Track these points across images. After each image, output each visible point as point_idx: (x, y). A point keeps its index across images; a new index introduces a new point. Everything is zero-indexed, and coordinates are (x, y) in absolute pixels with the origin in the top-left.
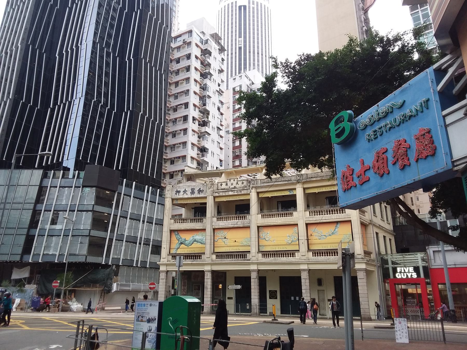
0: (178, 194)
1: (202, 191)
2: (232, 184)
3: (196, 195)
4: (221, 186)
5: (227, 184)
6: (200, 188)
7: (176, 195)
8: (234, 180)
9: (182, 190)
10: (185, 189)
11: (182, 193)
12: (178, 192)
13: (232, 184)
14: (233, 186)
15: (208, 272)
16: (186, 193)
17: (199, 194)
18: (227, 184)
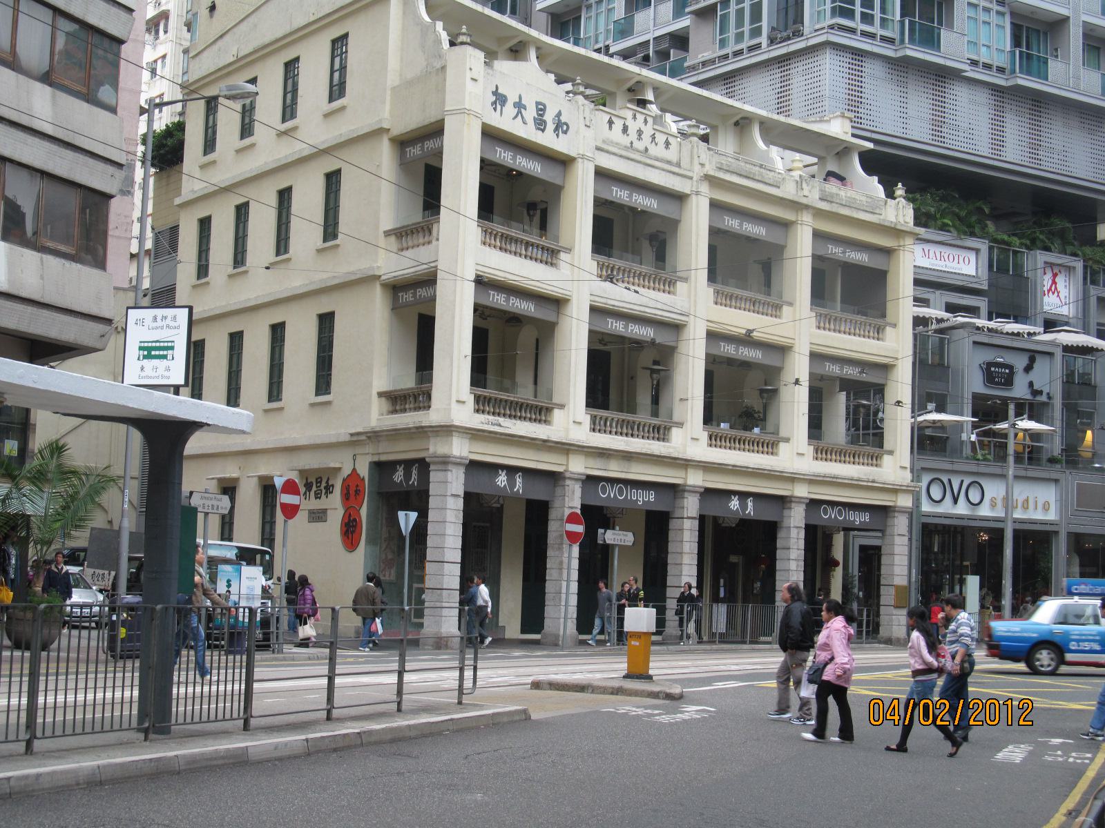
0: (499, 107)
1: (565, 128)
2: (640, 132)
3: (547, 139)
4: (610, 128)
5: (625, 129)
6: (559, 114)
7: (495, 109)
8: (646, 122)
9: (512, 99)
10: (520, 97)
11: (509, 109)
12: (499, 99)
13: (640, 132)
14: (639, 145)
15: (573, 482)
16: (522, 116)
17: (558, 135)
18: (625, 129)
